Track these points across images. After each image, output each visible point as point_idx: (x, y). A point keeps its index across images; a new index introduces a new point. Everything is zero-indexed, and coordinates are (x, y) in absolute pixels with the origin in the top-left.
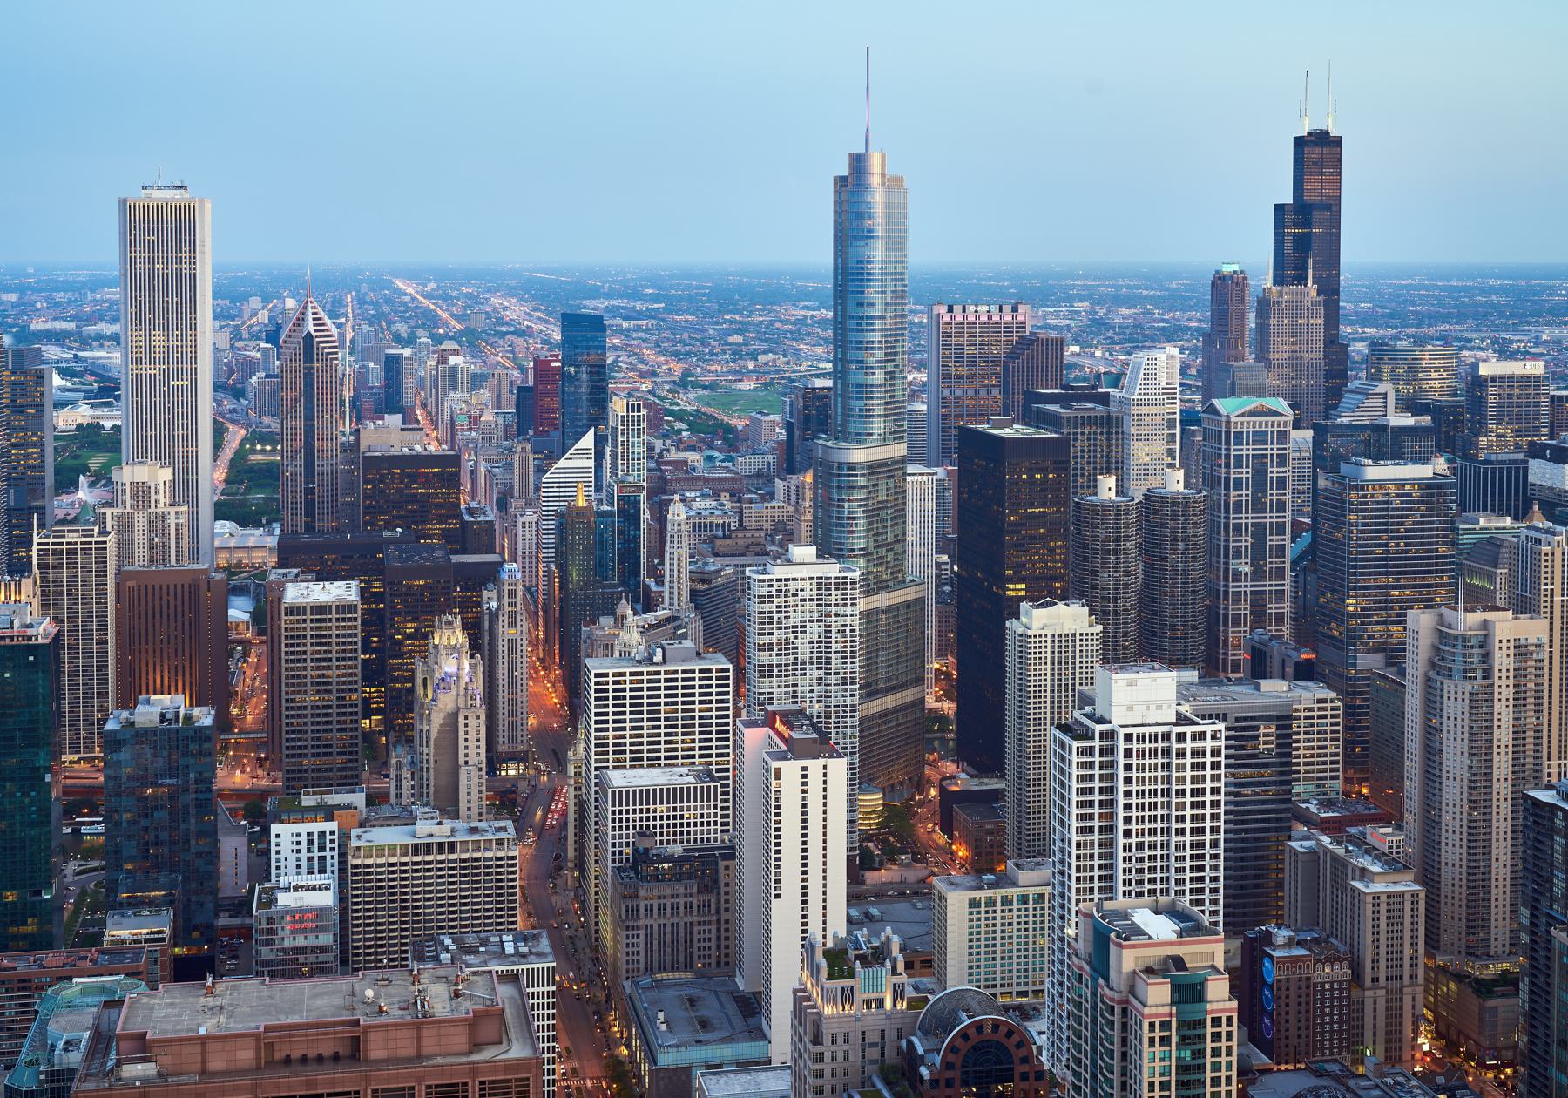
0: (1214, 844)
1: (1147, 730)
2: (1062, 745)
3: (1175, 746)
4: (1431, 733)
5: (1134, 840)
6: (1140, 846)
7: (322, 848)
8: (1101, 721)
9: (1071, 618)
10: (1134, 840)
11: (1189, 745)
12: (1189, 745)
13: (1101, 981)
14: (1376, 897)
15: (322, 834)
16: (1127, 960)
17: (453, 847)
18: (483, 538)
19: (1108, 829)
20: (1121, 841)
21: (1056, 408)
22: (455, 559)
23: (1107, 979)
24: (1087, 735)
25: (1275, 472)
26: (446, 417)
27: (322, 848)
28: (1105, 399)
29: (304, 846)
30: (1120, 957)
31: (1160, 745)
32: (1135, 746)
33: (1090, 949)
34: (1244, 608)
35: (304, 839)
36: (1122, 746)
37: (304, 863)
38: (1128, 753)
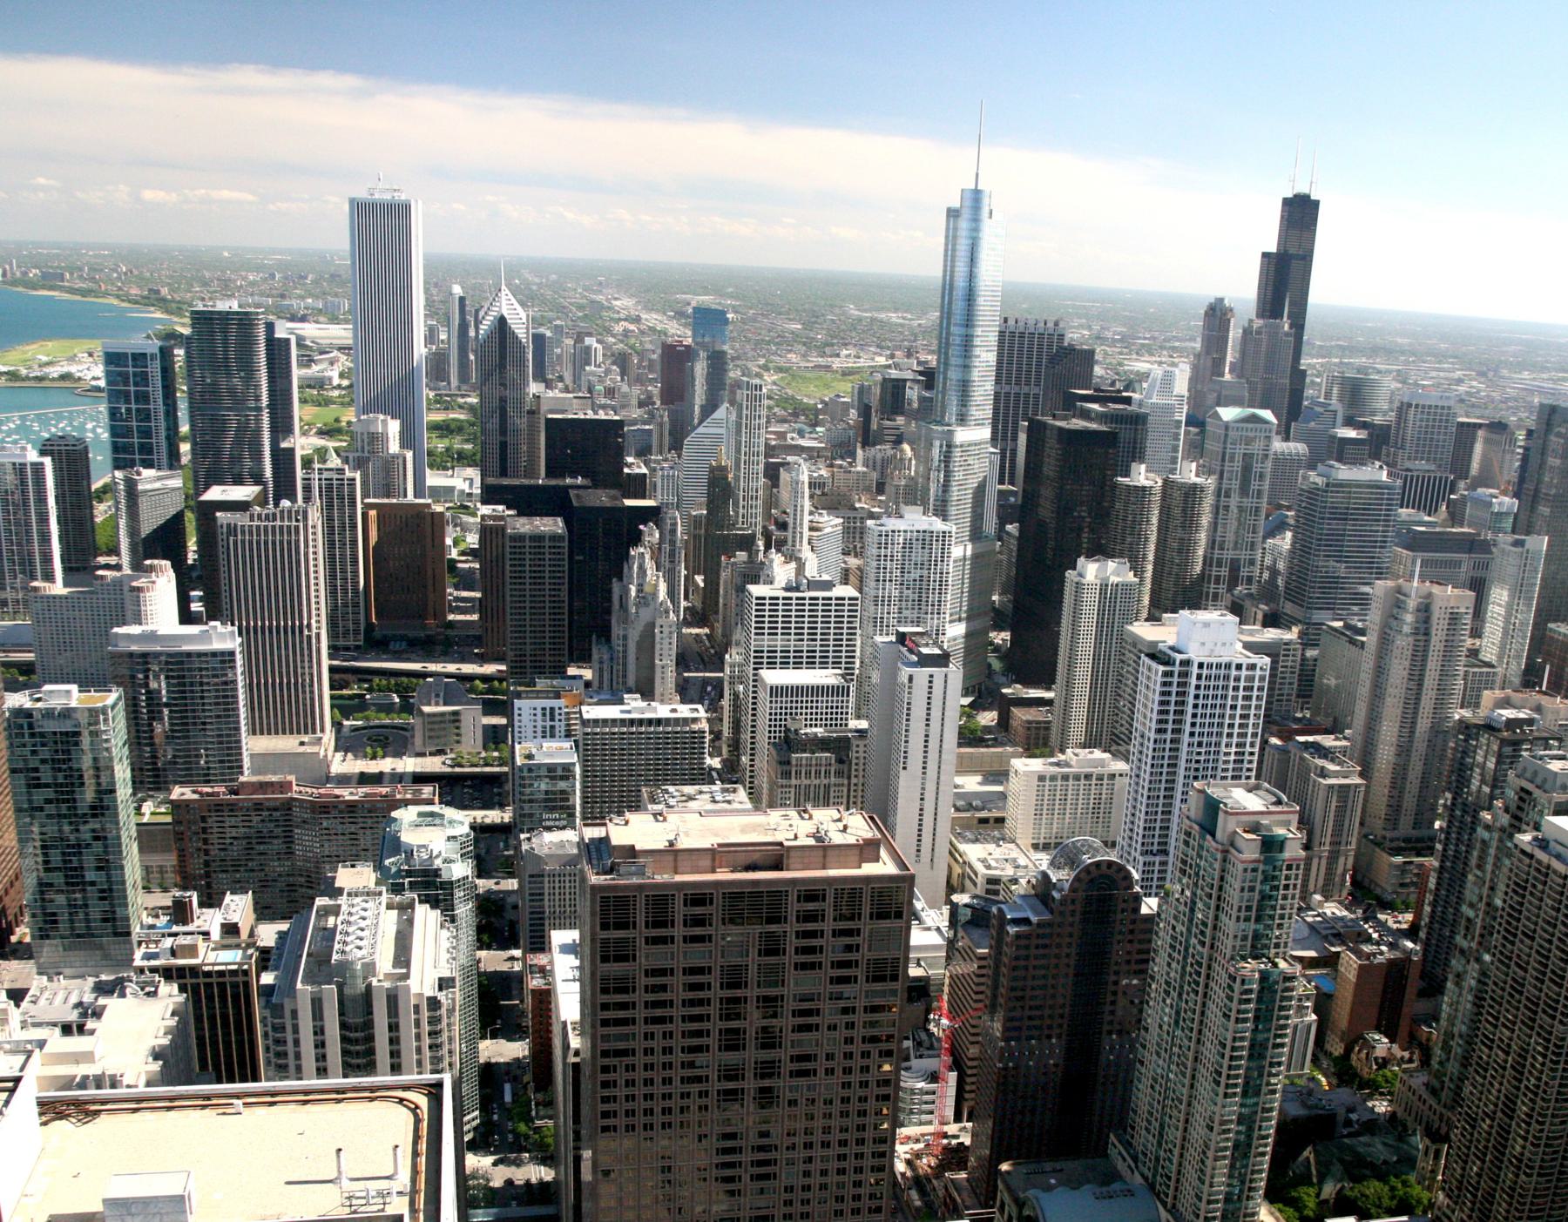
0: (1252, 745)
1: (1215, 660)
2: (1149, 669)
3: (1234, 673)
4: (1380, 671)
5: (1196, 739)
6: (1200, 744)
7: (552, 719)
8: (1180, 652)
9: (1114, 571)
10: (1196, 739)
11: (1244, 673)
12: (1244, 673)
13: (1209, 837)
14: (1331, 787)
15: (552, 709)
16: (1225, 826)
17: (659, 722)
18: (638, 486)
19: (1176, 731)
20: (1186, 738)
21: (1095, 406)
22: (629, 502)
23: (1213, 835)
24: (1168, 662)
25: (1257, 468)
26: (1238, 465)
27: (552, 719)
28: (1128, 401)
29: (539, 717)
30: (1225, 822)
31: (1223, 672)
32: (1205, 672)
33: (1200, 813)
34: (1225, 572)
35: (539, 712)
36: (1195, 670)
37: (539, 729)
38: (1199, 677)
